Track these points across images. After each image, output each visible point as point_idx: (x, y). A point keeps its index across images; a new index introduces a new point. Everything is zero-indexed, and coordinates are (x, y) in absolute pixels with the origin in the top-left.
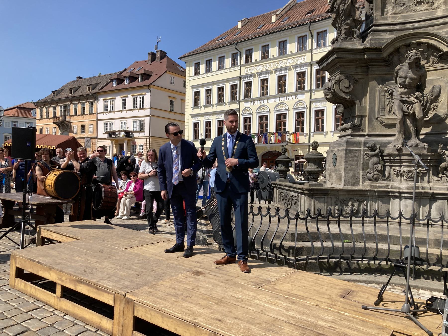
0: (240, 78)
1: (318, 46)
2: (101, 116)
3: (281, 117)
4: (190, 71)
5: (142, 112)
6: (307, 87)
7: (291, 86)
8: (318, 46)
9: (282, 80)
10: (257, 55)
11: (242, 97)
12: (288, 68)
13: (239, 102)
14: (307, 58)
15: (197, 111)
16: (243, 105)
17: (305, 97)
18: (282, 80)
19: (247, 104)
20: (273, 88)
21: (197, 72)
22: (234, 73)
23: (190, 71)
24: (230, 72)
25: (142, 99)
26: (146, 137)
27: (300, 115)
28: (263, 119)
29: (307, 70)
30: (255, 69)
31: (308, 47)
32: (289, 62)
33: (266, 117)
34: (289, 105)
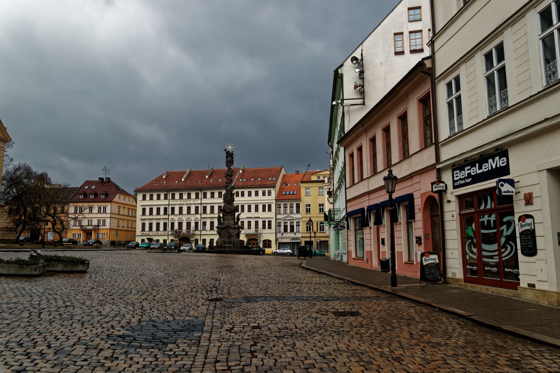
0: (169, 205)
1: (204, 198)
2: (70, 216)
3: (189, 224)
4: (140, 197)
5: (104, 215)
6: (200, 213)
7: (193, 211)
8: (204, 198)
9: (189, 209)
10: (177, 196)
11: (170, 213)
12: (192, 204)
13: (169, 215)
14: (199, 201)
15: (144, 217)
16: (170, 217)
17: (198, 216)
18: (189, 209)
19: (172, 216)
20: (185, 211)
21: (144, 198)
22: (166, 202)
23: (140, 197)
24: (163, 202)
25: (105, 209)
26: (107, 229)
27: (197, 224)
28: (180, 224)
29: (200, 206)
30: (176, 203)
31: (200, 197)
32: (192, 202)
33: (182, 223)
34: (193, 219)
